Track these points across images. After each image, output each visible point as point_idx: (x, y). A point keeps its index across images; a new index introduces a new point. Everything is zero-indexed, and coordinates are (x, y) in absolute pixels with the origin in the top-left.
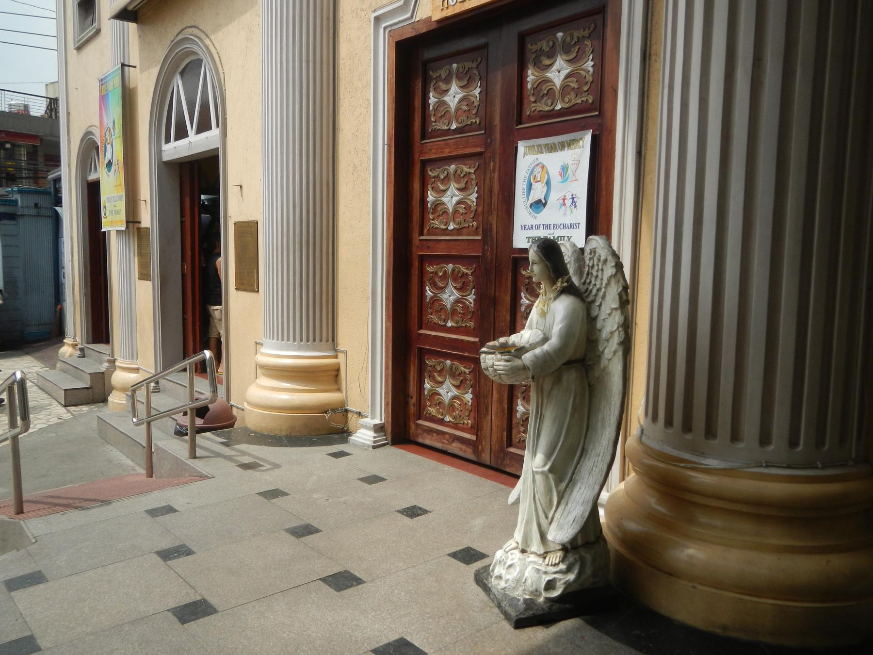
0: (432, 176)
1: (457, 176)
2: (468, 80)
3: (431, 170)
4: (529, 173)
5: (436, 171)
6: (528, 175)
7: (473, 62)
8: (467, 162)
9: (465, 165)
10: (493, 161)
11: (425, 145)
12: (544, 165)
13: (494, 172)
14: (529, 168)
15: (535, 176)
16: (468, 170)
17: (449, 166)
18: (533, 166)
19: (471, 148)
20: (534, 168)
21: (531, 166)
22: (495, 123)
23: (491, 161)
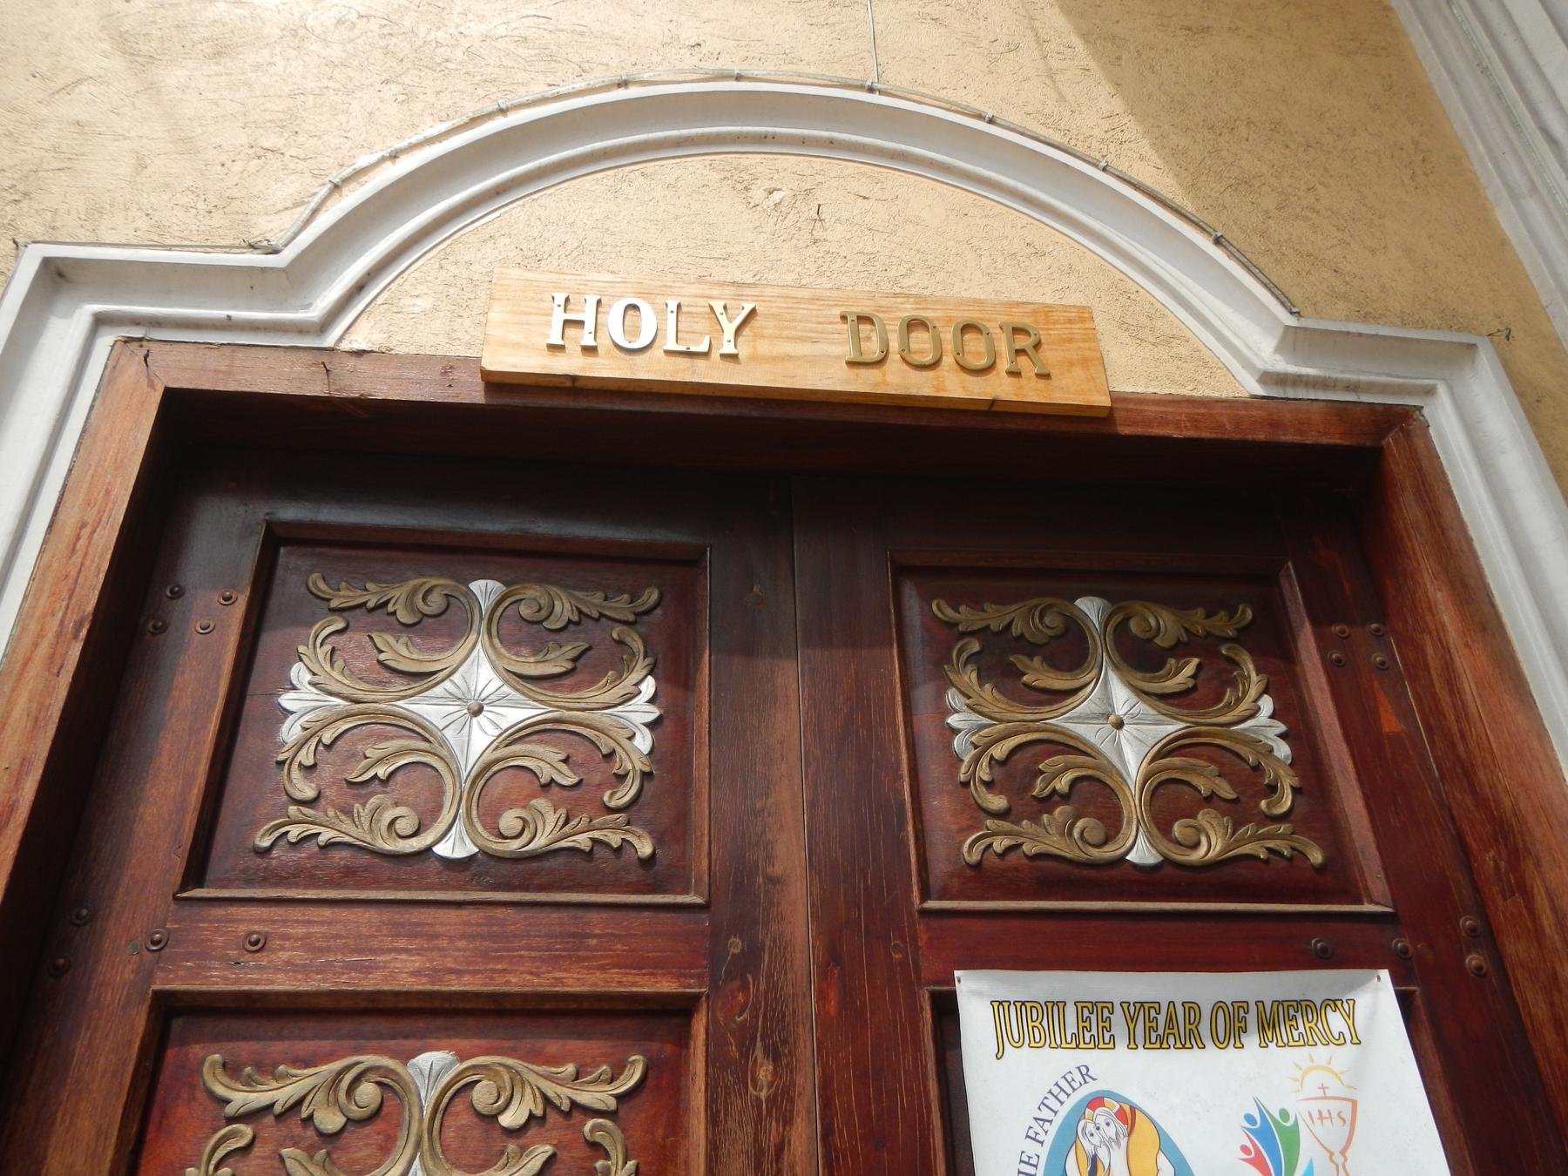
0: (230, 1110)
1: (461, 1118)
2: (575, 660)
3: (232, 1069)
4: (1049, 1140)
5: (277, 1078)
6: (1044, 1152)
7: (606, 599)
8: (553, 1047)
9: (535, 1057)
10: (775, 1055)
11: (219, 912)
12: (1133, 1109)
13: (788, 1121)
14: (1046, 1114)
15: (1094, 1160)
16: (563, 1094)
17: (406, 1057)
18: (1070, 1103)
19: (602, 968)
20: (1077, 1114)
21: (1052, 1102)
22: (777, 869)
23: (759, 1052)
